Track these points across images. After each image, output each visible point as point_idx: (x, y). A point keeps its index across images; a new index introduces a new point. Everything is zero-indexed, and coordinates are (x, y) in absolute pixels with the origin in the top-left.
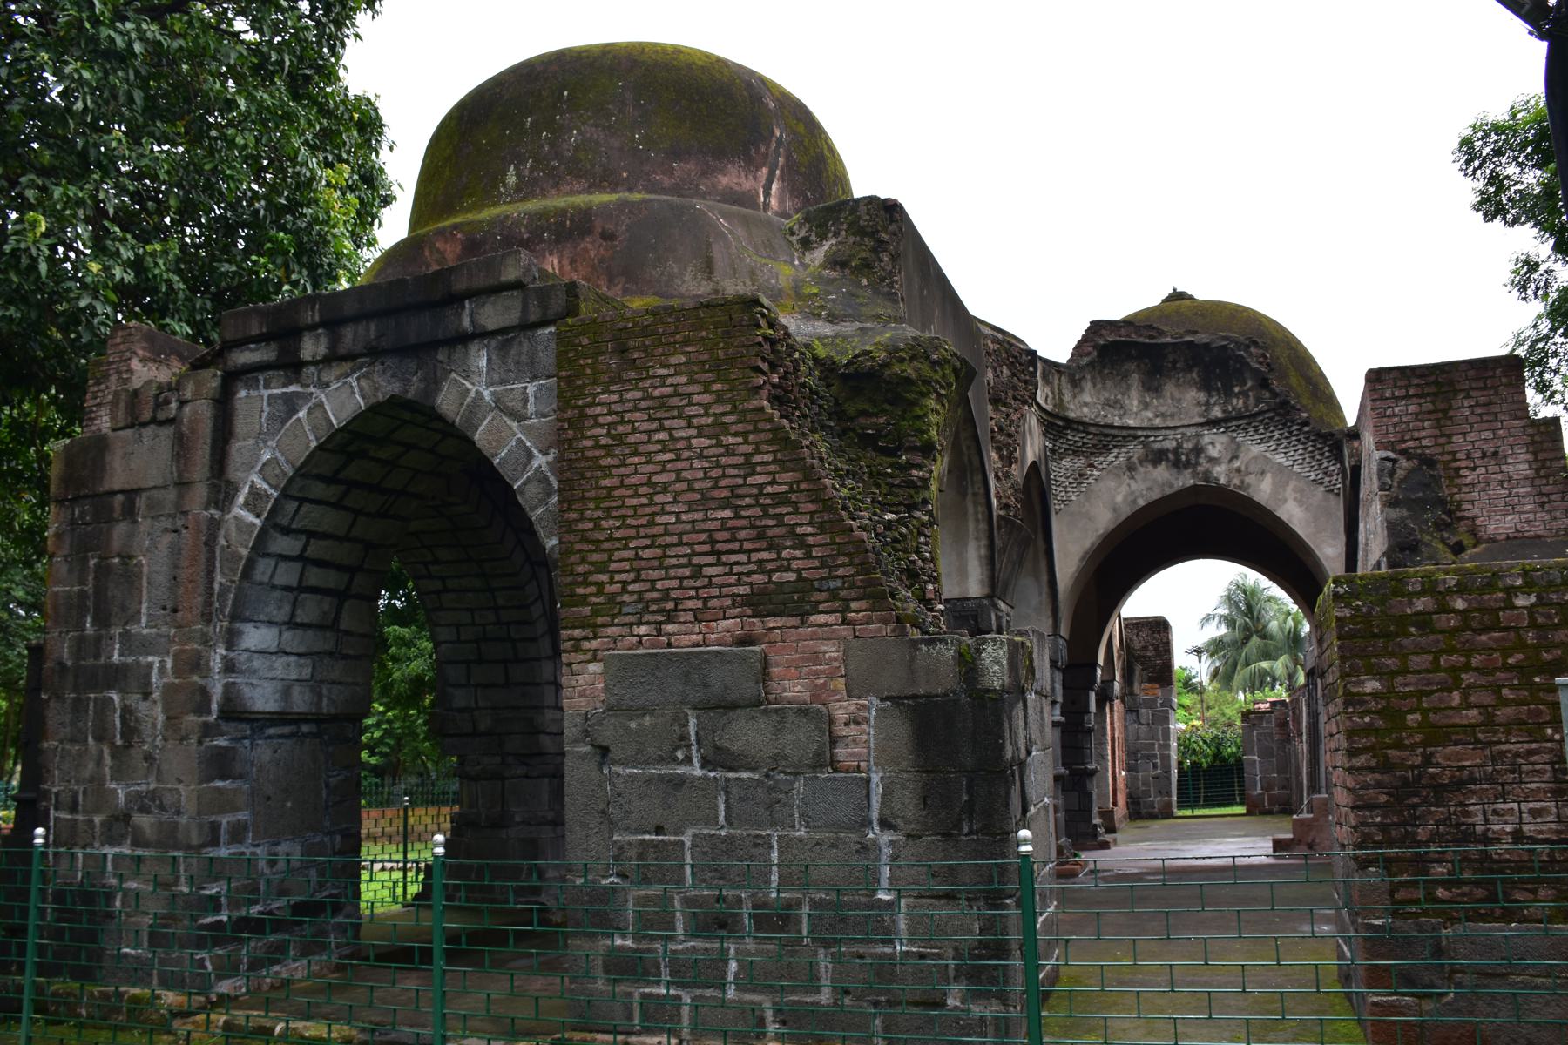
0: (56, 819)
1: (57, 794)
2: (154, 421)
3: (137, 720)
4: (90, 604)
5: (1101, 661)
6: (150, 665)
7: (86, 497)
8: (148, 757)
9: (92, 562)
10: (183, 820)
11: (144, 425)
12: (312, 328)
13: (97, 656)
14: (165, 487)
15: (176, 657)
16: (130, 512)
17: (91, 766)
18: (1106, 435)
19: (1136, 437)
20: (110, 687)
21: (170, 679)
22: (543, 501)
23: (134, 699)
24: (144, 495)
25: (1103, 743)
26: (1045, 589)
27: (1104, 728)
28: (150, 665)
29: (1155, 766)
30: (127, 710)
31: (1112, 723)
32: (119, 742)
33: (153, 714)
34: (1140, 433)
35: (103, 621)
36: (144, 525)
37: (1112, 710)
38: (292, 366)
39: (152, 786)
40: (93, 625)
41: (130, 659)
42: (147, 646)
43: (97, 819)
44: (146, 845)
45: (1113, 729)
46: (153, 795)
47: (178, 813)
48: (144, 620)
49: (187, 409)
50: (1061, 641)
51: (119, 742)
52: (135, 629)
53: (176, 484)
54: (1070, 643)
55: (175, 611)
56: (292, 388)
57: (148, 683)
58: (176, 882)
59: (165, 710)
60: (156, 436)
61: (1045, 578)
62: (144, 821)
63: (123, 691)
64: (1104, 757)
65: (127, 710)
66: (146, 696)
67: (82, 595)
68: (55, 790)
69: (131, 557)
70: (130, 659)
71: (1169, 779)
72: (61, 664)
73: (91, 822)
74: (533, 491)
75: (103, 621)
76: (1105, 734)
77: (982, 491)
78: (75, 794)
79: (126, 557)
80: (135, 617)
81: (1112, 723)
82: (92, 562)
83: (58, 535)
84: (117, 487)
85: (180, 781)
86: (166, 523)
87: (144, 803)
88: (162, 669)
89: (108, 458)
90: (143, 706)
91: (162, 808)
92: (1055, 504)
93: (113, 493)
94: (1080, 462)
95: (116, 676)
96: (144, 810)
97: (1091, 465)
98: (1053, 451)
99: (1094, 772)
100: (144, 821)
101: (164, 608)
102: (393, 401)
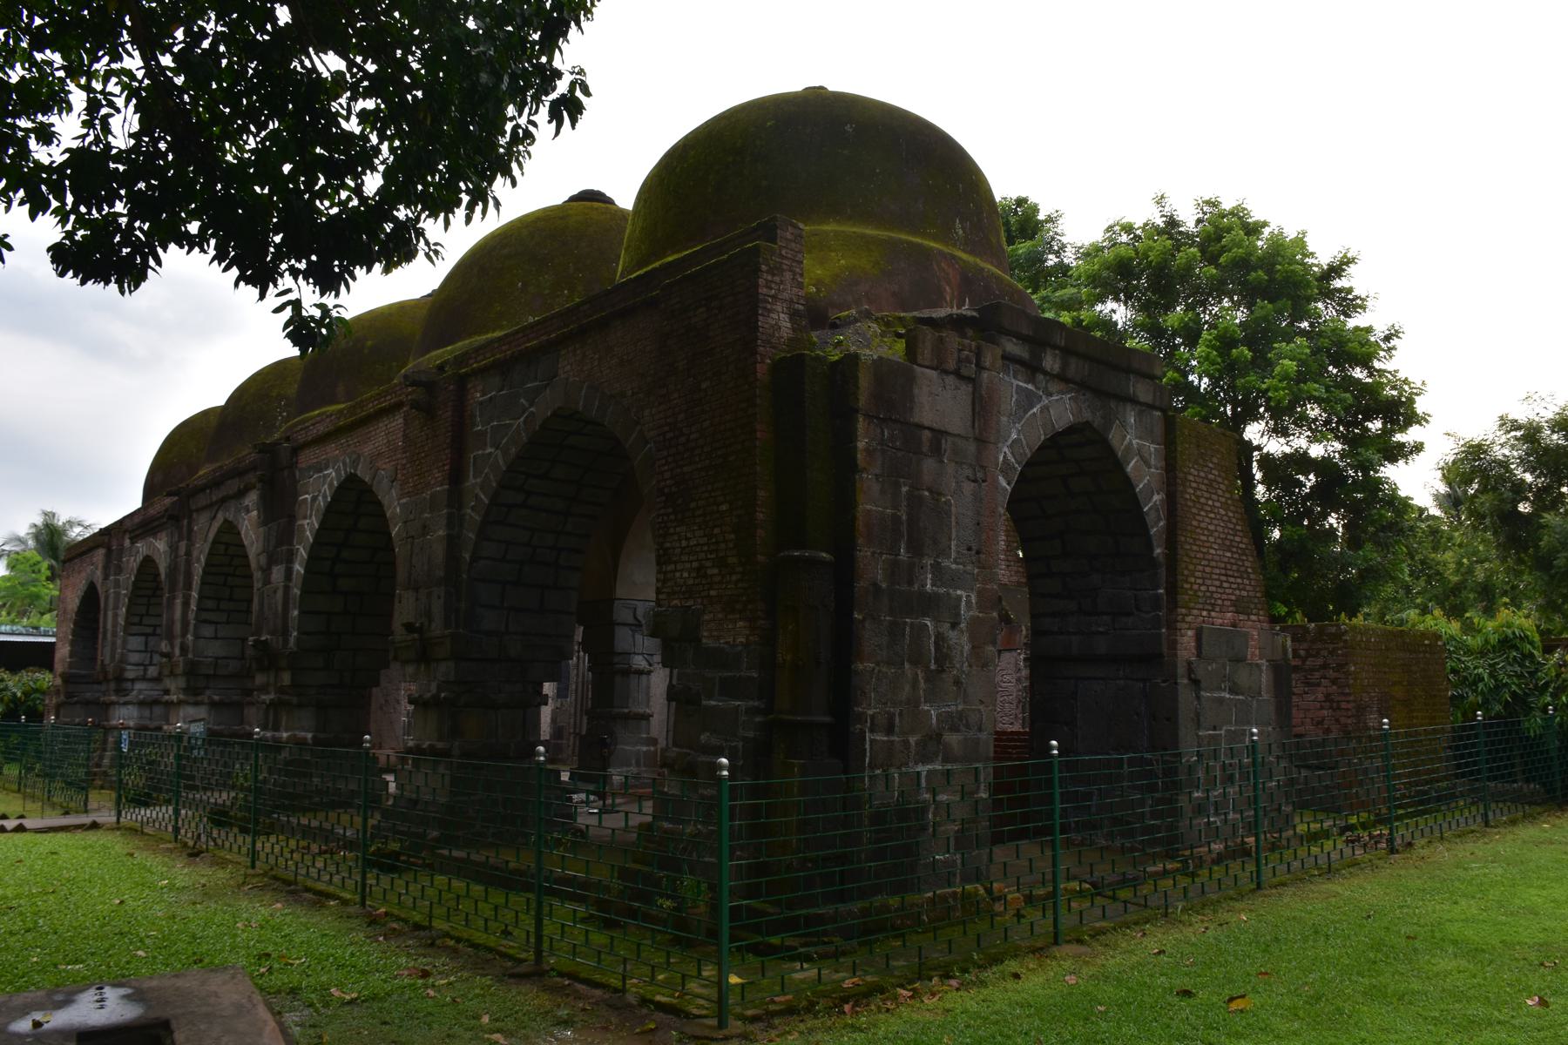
0: (872, 741)
1: (873, 717)
2: (957, 374)
3: (949, 647)
4: (904, 528)
6: (960, 597)
7: (896, 421)
8: (957, 682)
9: (905, 489)
10: (984, 736)
11: (946, 372)
12: (1054, 347)
13: (910, 583)
14: (967, 439)
15: (980, 594)
16: (936, 450)
17: (907, 688)
20: (925, 615)
21: (974, 613)
22: (1156, 524)
23: (945, 628)
24: (950, 439)
28: (960, 597)
30: (940, 638)
32: (933, 667)
33: (960, 641)
35: (916, 549)
36: (950, 468)
38: (1032, 368)
39: (960, 707)
40: (908, 550)
41: (942, 590)
42: (955, 580)
43: (912, 740)
44: (955, 761)
46: (961, 715)
47: (980, 730)
48: (953, 555)
49: (985, 375)
51: (933, 667)
52: (946, 563)
53: (976, 439)
55: (978, 553)
56: (1030, 387)
57: (958, 614)
58: (977, 790)
59: (972, 639)
60: (957, 388)
62: (952, 739)
63: (937, 620)
65: (940, 638)
66: (954, 626)
67: (896, 519)
68: (870, 712)
69: (940, 494)
70: (942, 590)
72: (875, 584)
73: (906, 743)
74: (1153, 515)
75: (916, 549)
78: (891, 717)
79: (936, 493)
80: (945, 553)
82: (905, 489)
83: (869, 452)
84: (926, 424)
85: (982, 702)
86: (968, 472)
87: (955, 722)
88: (968, 602)
89: (916, 391)
90: (952, 634)
91: (968, 726)
93: (922, 427)
95: (929, 604)
96: (954, 729)
100: (952, 739)
101: (969, 549)
102: (1087, 424)
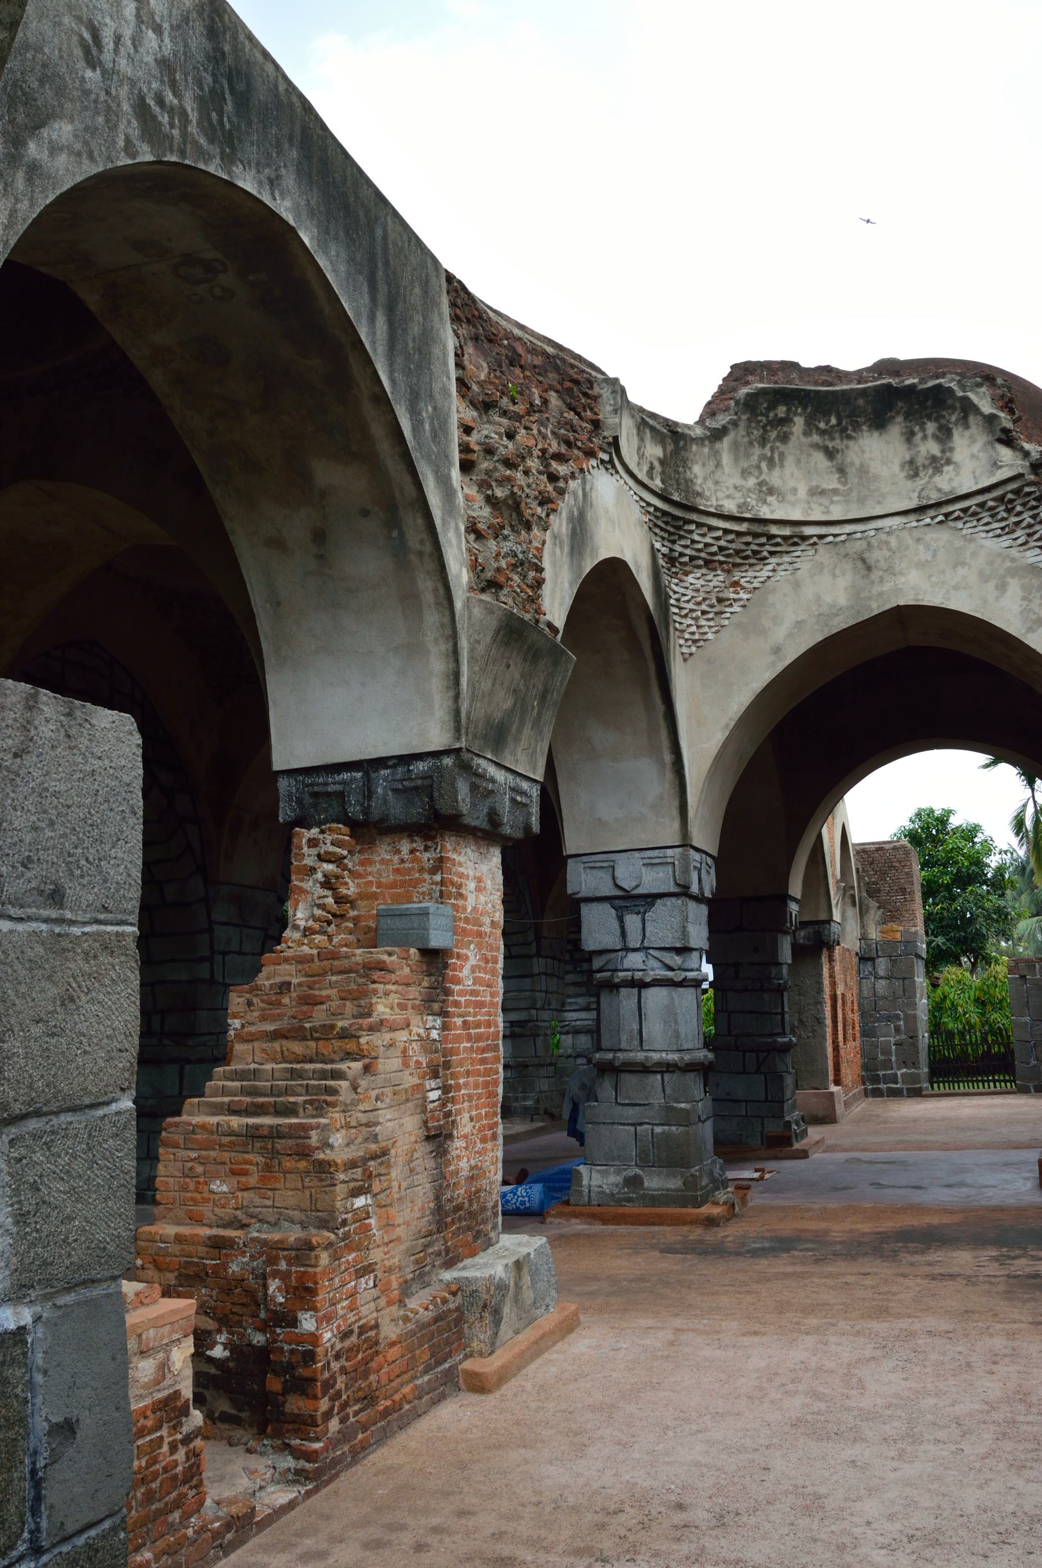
5: (796, 889)
18: (756, 535)
19: (805, 538)
25: (819, 1003)
26: (669, 775)
27: (820, 983)
29: (897, 1029)
31: (832, 976)
34: (808, 531)
37: (831, 960)
45: (833, 984)
50: (697, 856)
54: (723, 862)
61: (668, 758)
64: (820, 1022)
71: (915, 1046)
76: (820, 991)
77: (428, 548)
81: (832, 976)
92: (677, 648)
94: (718, 579)
97: (736, 584)
98: (672, 560)
99: (787, 1048)
